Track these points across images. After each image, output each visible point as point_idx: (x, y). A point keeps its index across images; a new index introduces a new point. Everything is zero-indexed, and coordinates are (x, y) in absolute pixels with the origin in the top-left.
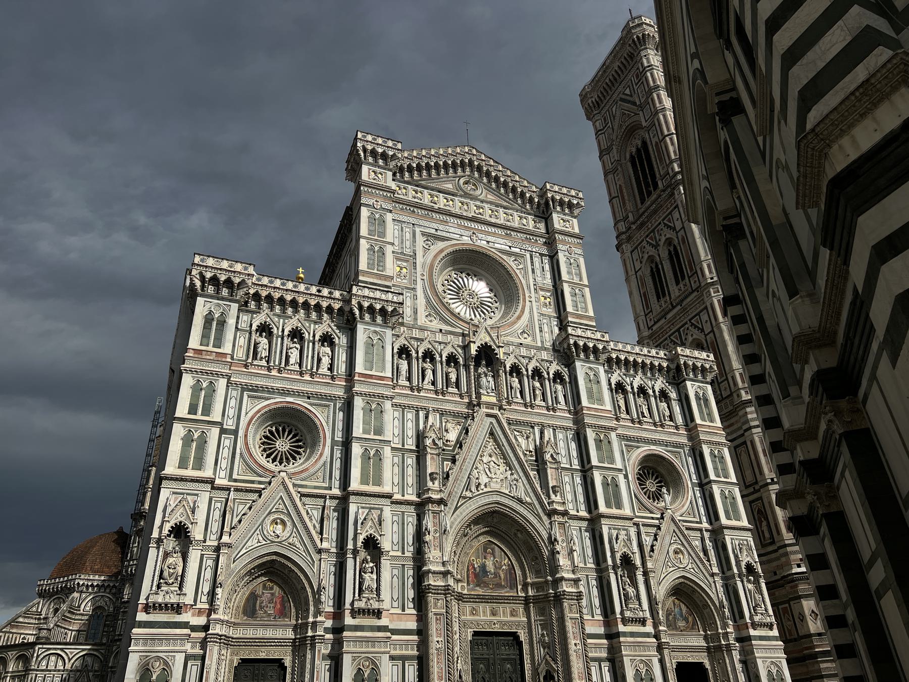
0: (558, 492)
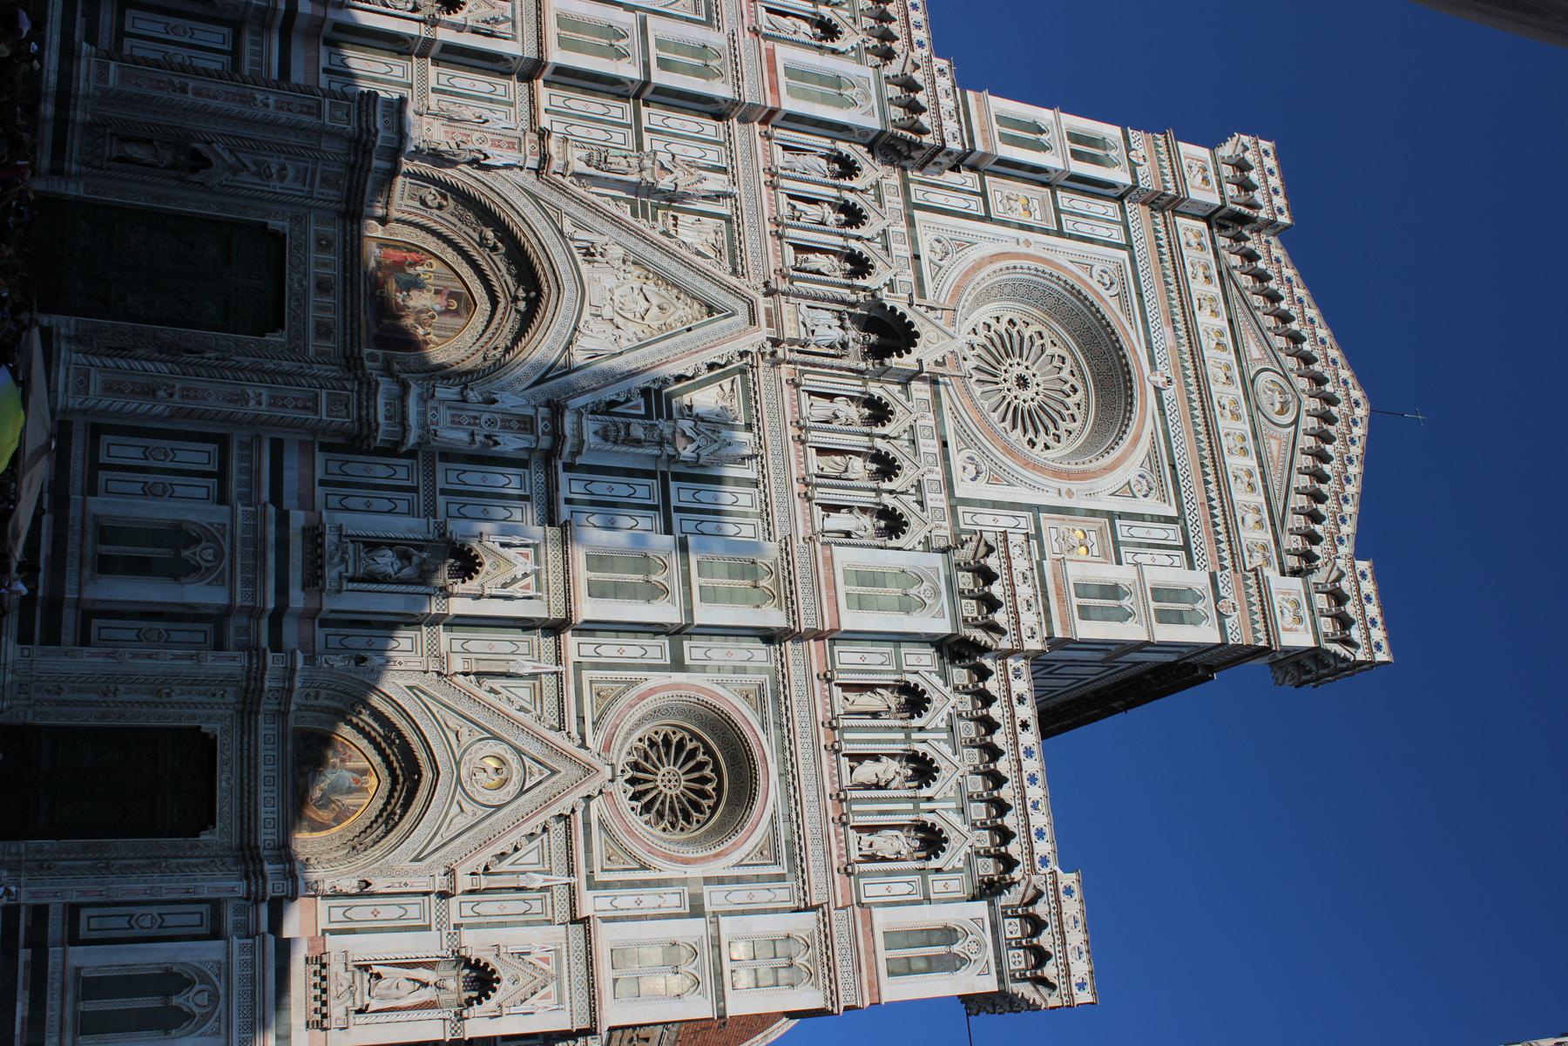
0: (605, 438)
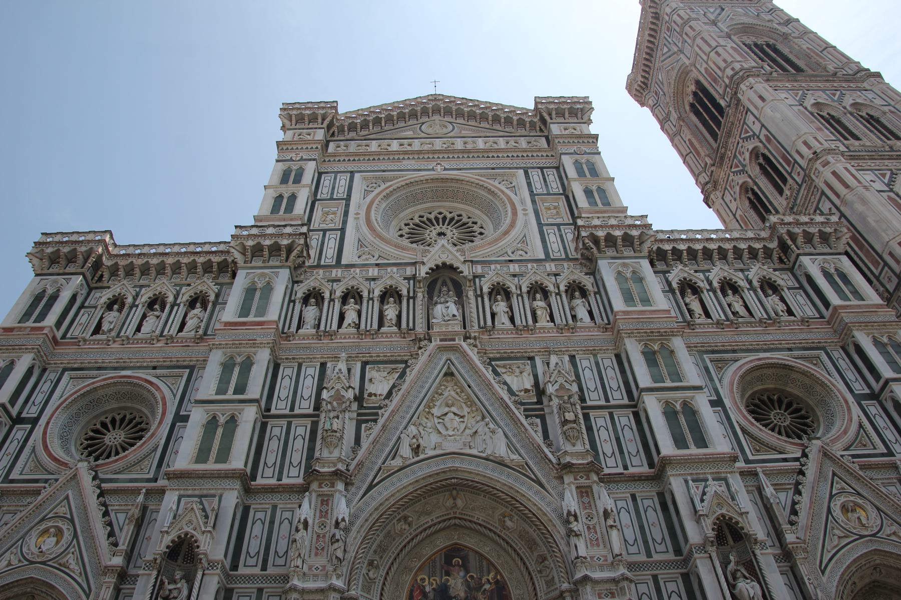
0: (577, 438)
